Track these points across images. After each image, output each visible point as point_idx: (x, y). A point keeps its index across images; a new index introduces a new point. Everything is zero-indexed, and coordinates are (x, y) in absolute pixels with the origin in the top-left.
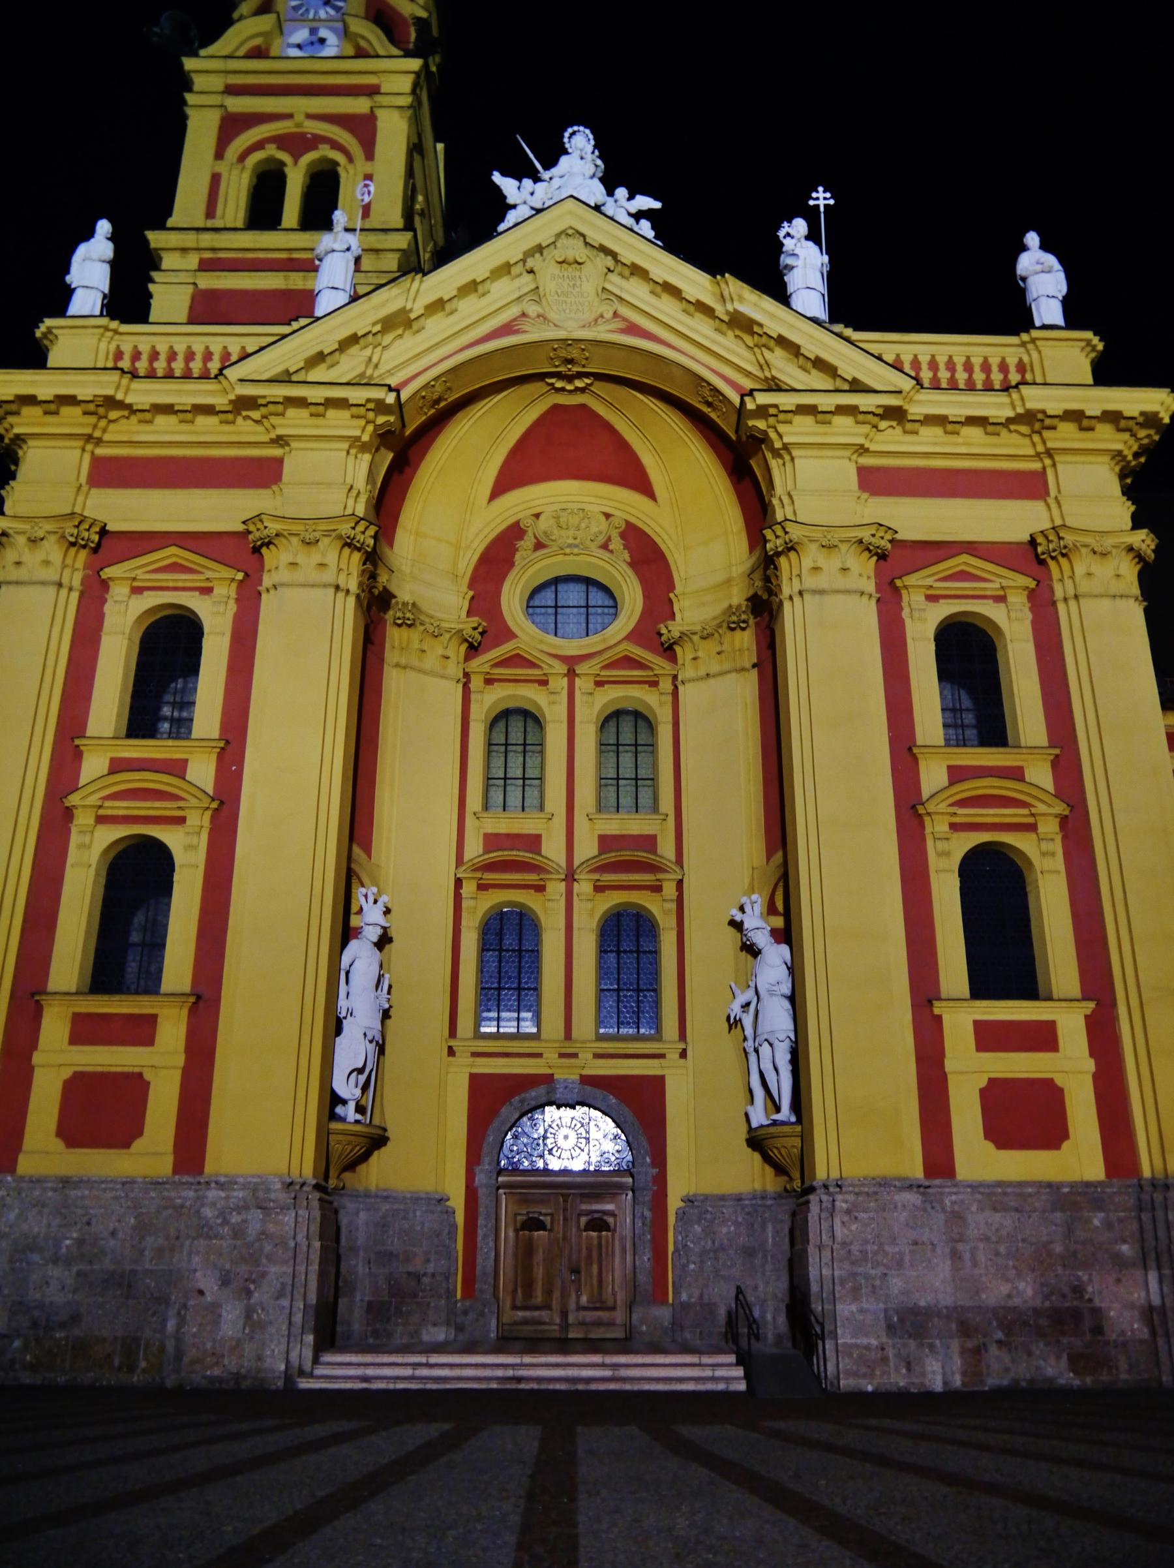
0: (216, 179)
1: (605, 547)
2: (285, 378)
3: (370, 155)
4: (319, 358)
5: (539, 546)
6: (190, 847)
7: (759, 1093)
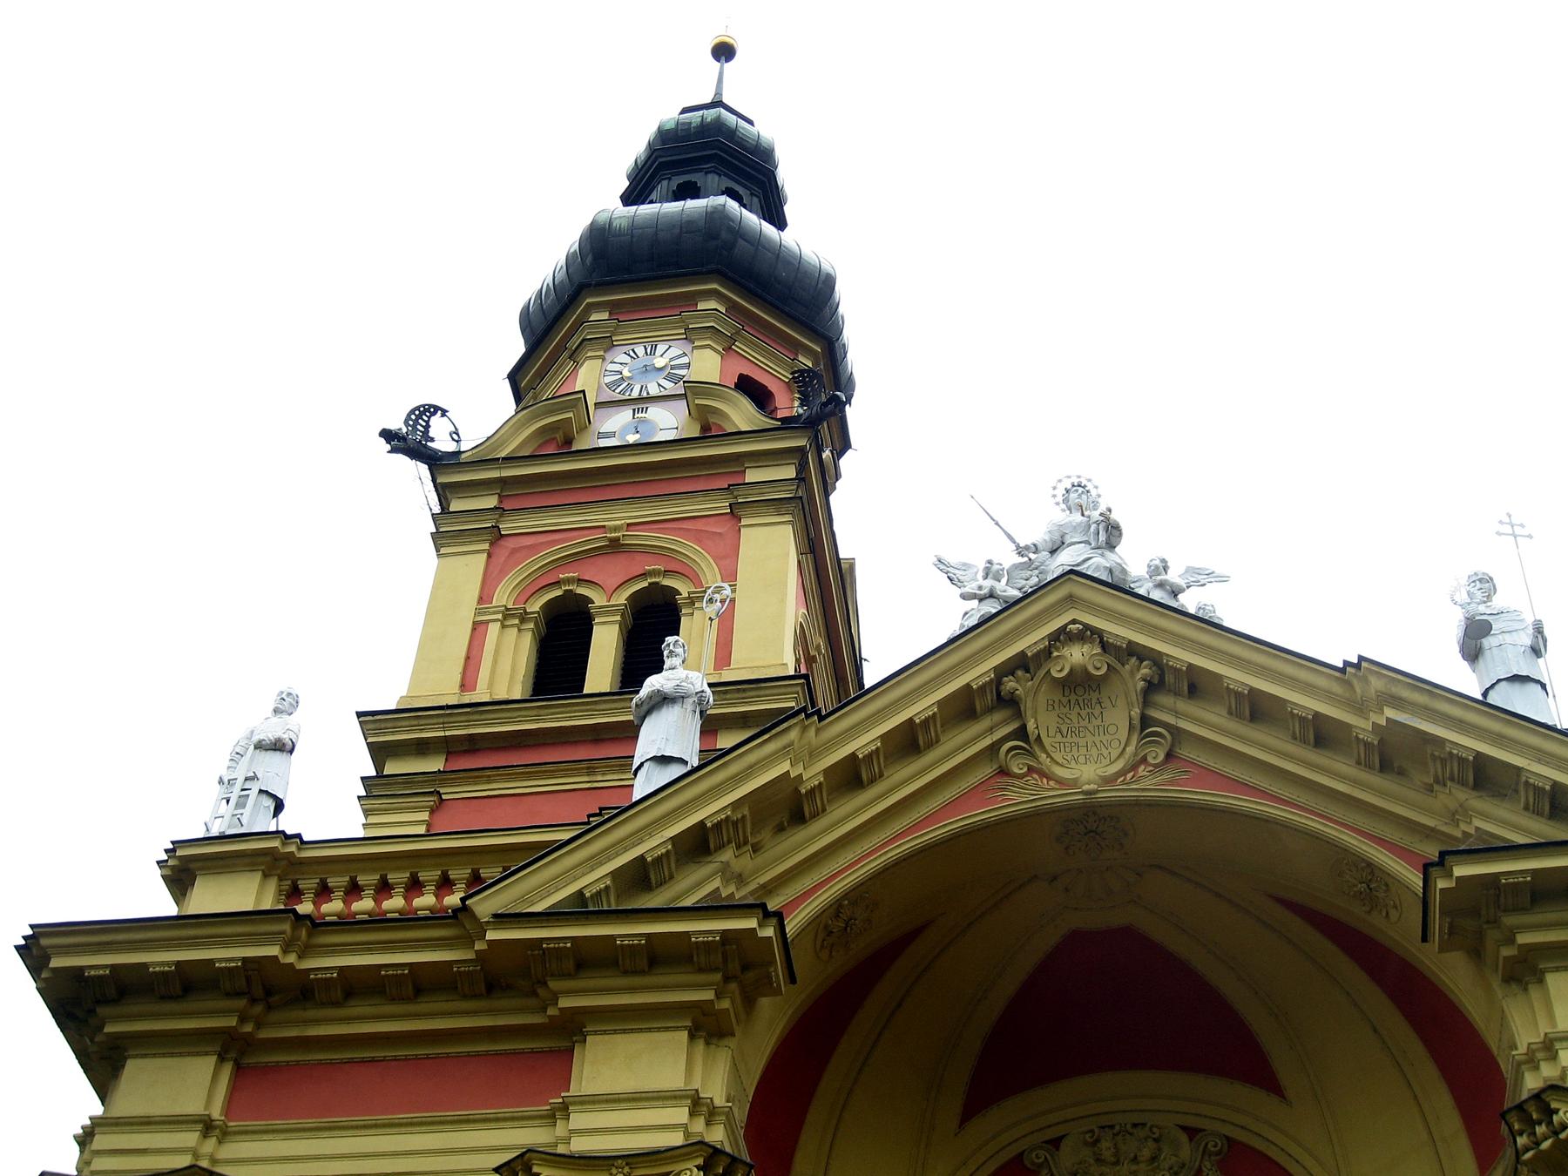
0: (478, 628)
2: (579, 909)
3: (730, 576)
4: (640, 876)
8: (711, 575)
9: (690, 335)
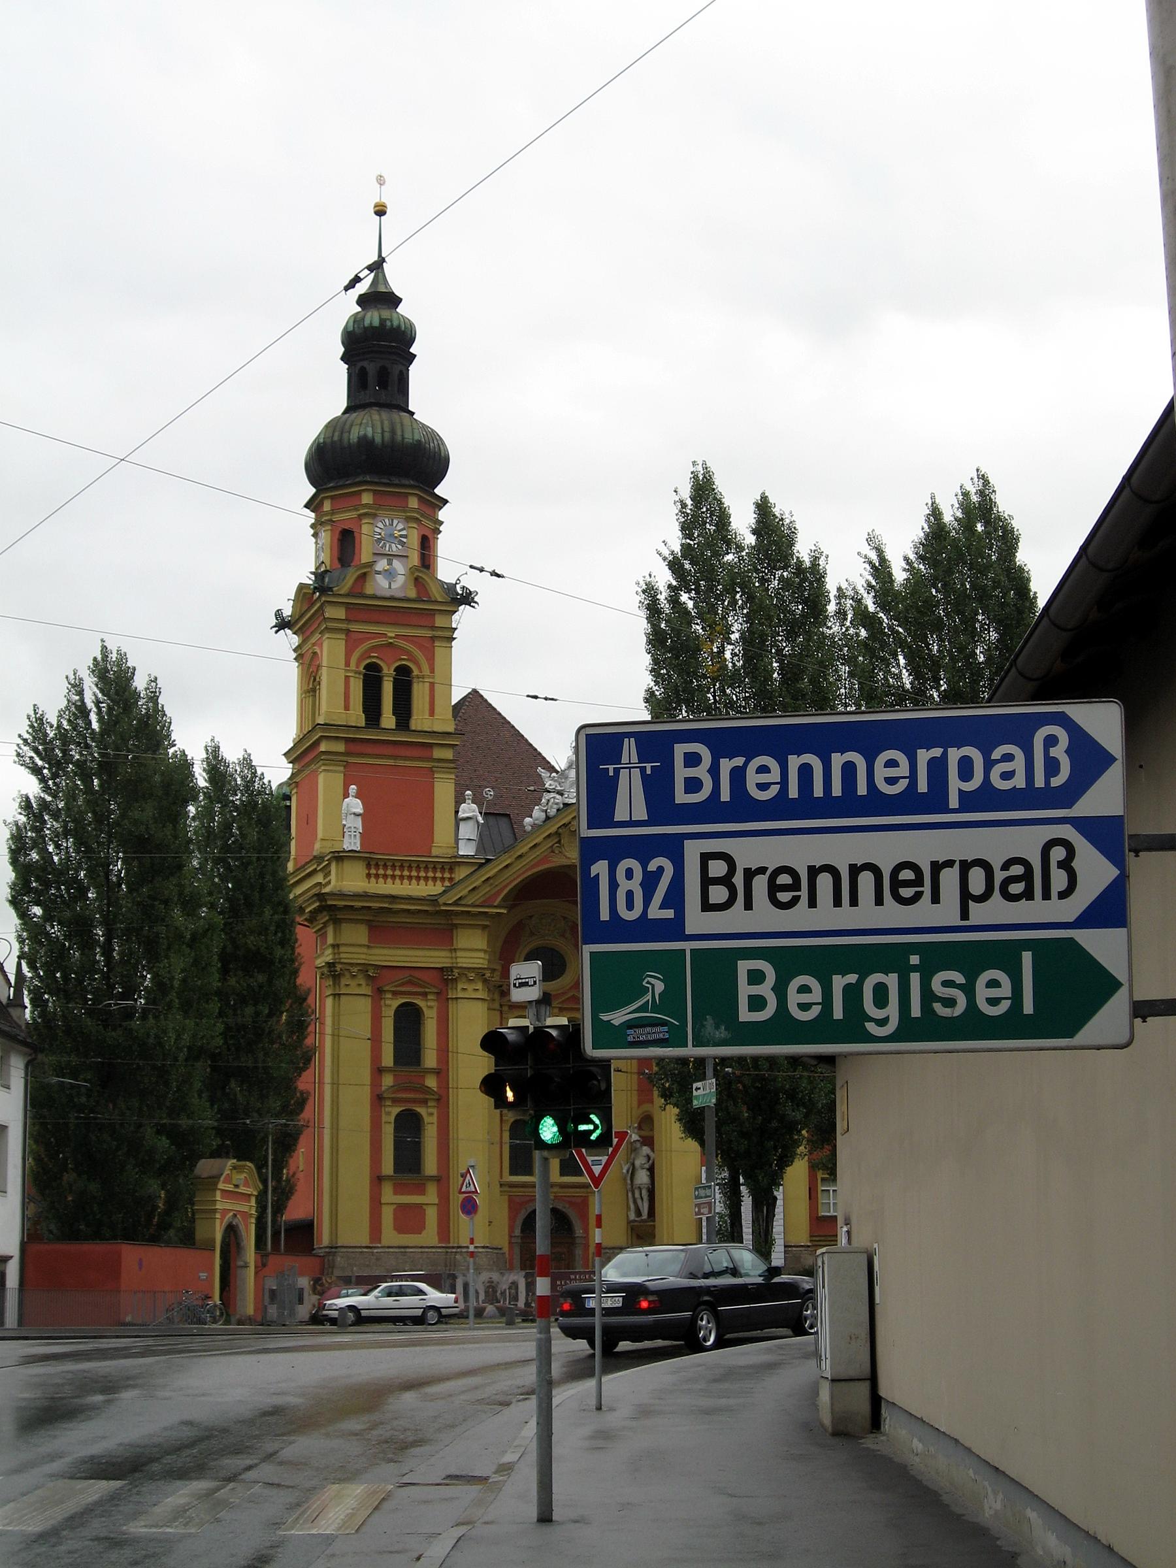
0: (347, 678)
1: (563, 936)
3: (432, 671)
5: (532, 934)
6: (431, 1114)
7: (632, 1206)
8: (426, 670)
9: (408, 519)
